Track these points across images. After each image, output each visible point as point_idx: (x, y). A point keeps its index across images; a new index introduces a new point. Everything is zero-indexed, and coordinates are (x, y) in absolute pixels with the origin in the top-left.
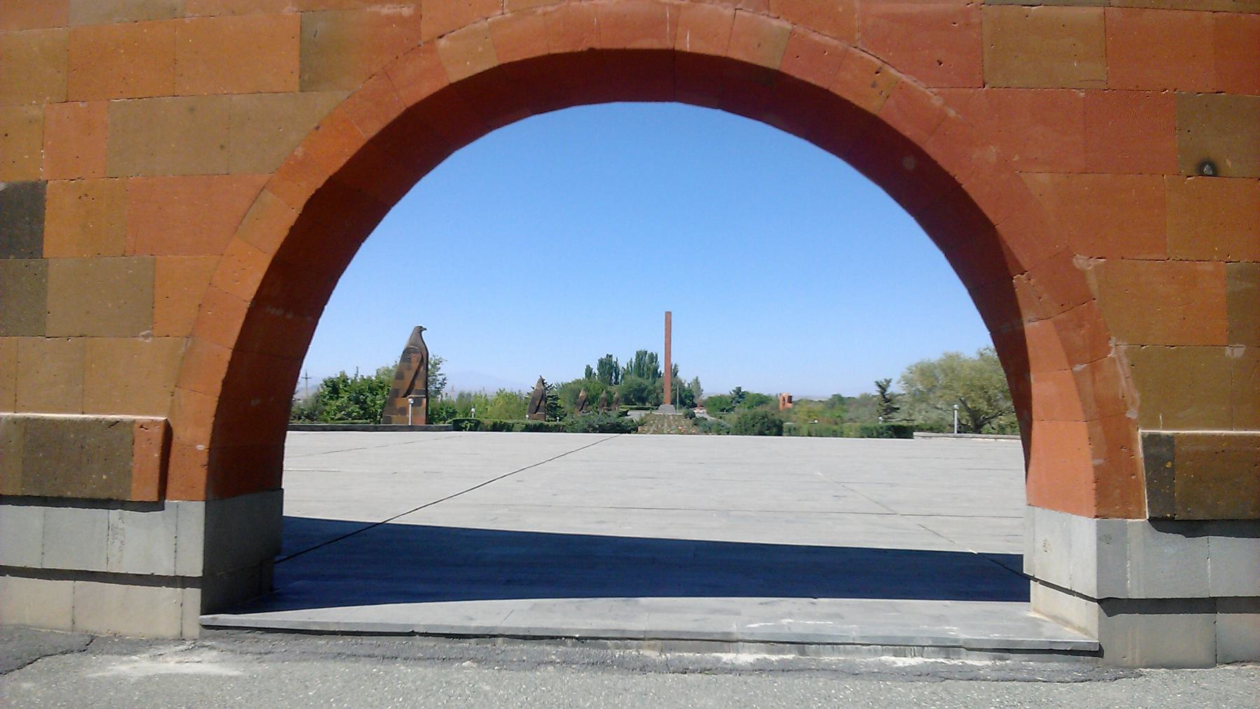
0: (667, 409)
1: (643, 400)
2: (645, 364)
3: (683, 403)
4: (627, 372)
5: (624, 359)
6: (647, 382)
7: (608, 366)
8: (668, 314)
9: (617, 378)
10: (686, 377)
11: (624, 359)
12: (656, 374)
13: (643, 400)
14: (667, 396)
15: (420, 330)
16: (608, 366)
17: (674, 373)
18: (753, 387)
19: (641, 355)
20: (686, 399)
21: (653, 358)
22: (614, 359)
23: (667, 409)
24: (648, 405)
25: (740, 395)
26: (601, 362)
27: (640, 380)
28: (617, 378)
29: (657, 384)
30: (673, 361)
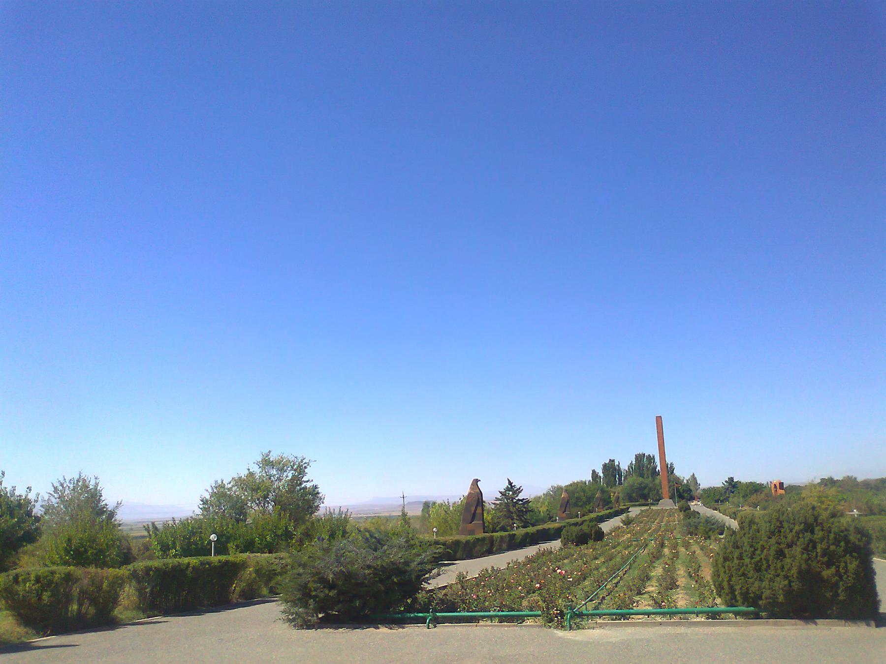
0: (667, 504)
1: (645, 497)
2: (643, 464)
3: (681, 497)
4: (629, 473)
5: (625, 462)
6: (648, 481)
7: (611, 469)
8: (659, 420)
9: (620, 479)
10: (682, 473)
11: (625, 462)
12: (655, 473)
13: (645, 497)
14: (665, 491)
15: (476, 481)
16: (611, 469)
17: (670, 470)
18: (743, 477)
19: (639, 458)
20: (684, 492)
21: (651, 459)
22: (617, 463)
23: (667, 504)
24: (650, 501)
25: (732, 485)
26: (605, 466)
27: (641, 479)
28: (620, 479)
29: (657, 481)
30: (668, 461)
